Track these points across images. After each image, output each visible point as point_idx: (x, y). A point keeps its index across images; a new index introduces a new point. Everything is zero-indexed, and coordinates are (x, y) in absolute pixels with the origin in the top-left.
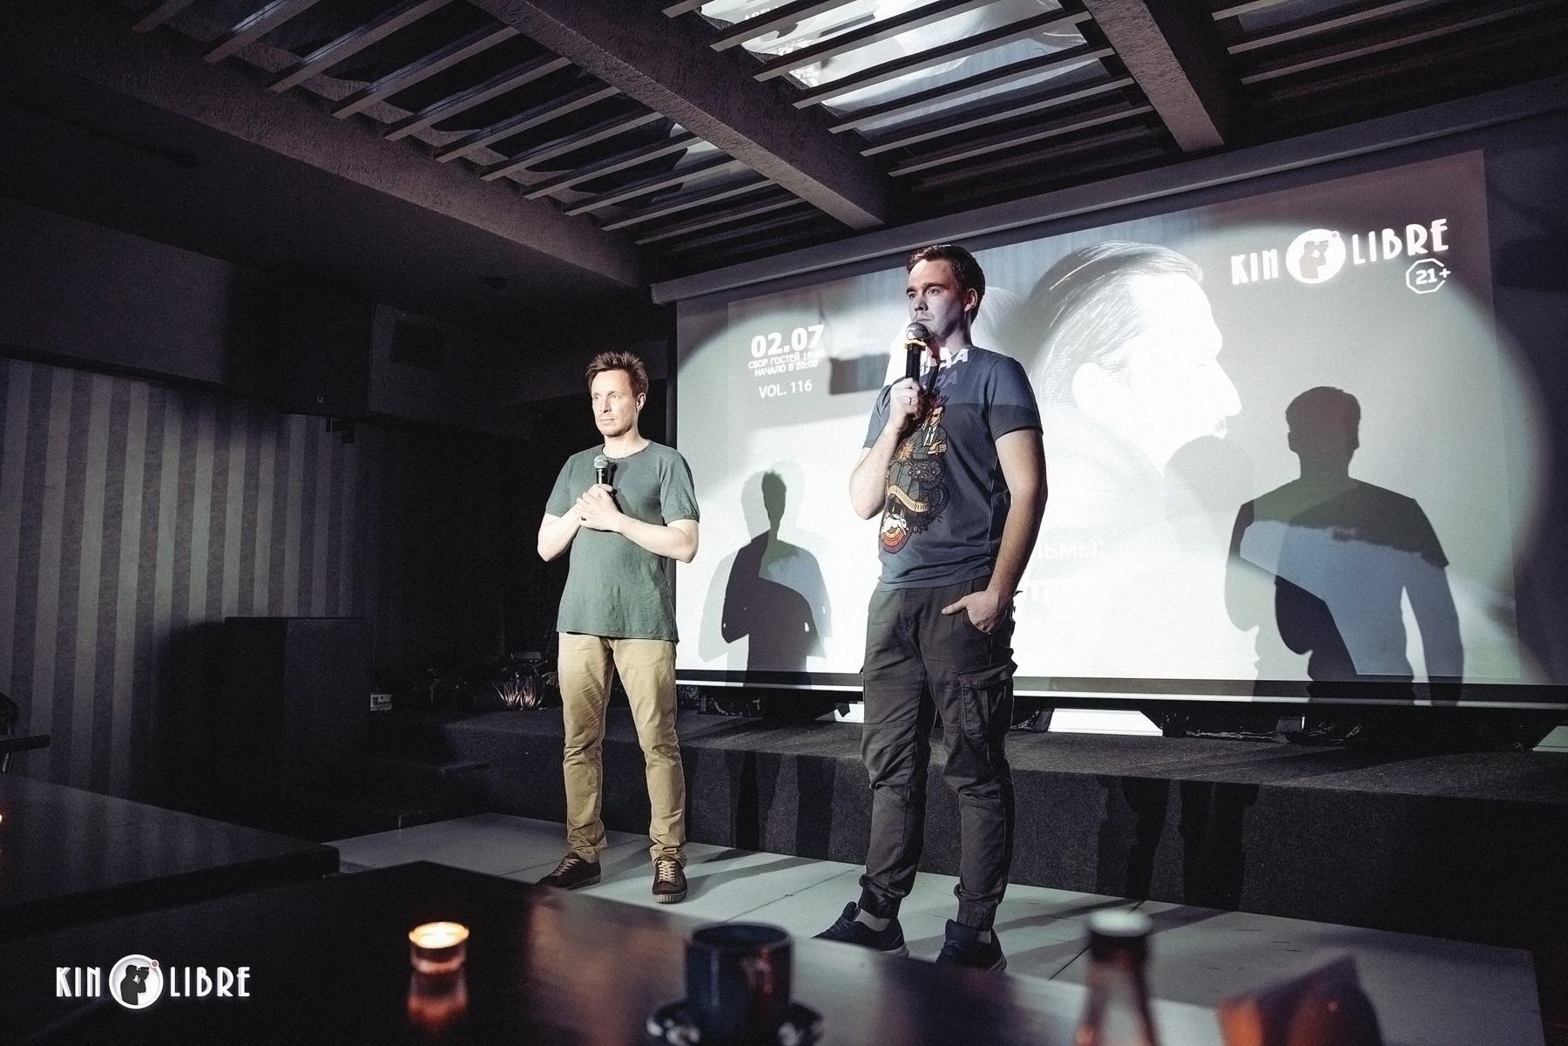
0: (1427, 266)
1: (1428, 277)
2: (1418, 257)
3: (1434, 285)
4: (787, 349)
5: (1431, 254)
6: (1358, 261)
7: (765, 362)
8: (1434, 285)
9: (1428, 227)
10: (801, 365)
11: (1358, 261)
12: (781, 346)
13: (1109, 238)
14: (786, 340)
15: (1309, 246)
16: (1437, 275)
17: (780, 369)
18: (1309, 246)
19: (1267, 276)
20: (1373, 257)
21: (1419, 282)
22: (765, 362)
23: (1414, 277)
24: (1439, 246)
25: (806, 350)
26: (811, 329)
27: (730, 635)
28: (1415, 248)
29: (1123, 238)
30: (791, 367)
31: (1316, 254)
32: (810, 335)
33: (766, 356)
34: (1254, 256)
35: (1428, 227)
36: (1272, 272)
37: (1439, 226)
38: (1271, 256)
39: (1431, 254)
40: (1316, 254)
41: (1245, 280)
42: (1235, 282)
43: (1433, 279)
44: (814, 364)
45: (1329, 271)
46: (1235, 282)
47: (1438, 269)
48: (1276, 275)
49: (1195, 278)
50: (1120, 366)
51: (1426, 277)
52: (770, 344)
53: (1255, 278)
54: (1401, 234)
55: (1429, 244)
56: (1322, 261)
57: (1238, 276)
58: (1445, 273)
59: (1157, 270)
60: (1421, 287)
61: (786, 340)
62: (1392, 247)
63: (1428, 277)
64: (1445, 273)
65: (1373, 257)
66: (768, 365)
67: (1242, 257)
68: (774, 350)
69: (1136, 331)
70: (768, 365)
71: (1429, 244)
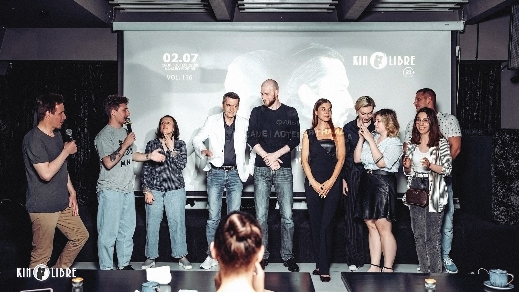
0: (409, 69)
1: (409, 73)
2: (407, 66)
3: (410, 75)
4: (181, 61)
7: (170, 65)
8: (410, 75)
9: (410, 58)
10: (187, 69)
11: (391, 64)
12: (178, 59)
14: (180, 57)
15: (377, 57)
16: (412, 74)
17: (178, 69)
18: (377, 57)
19: (364, 64)
20: (395, 64)
21: (406, 74)
22: (170, 65)
23: (405, 72)
24: (412, 64)
25: (190, 63)
26: (192, 54)
28: (406, 63)
30: (182, 69)
31: (379, 60)
32: (192, 57)
33: (170, 62)
34: (360, 57)
35: (410, 58)
36: (365, 63)
37: (413, 58)
39: (410, 66)
40: (379, 60)
41: (357, 64)
42: (354, 64)
43: (410, 74)
44: (193, 69)
45: (382, 66)
46: (354, 64)
47: (412, 71)
48: (367, 64)
49: (342, 61)
50: (315, 87)
51: (408, 72)
52: (172, 58)
53: (360, 64)
54: (403, 58)
55: (410, 63)
56: (380, 62)
57: (355, 62)
58: (413, 72)
59: (330, 56)
60: (407, 75)
61: (180, 57)
62: (400, 61)
63: (409, 73)
64: (413, 72)
66: (171, 67)
68: (174, 61)
69: (322, 76)
70: (171, 67)
71: (410, 63)
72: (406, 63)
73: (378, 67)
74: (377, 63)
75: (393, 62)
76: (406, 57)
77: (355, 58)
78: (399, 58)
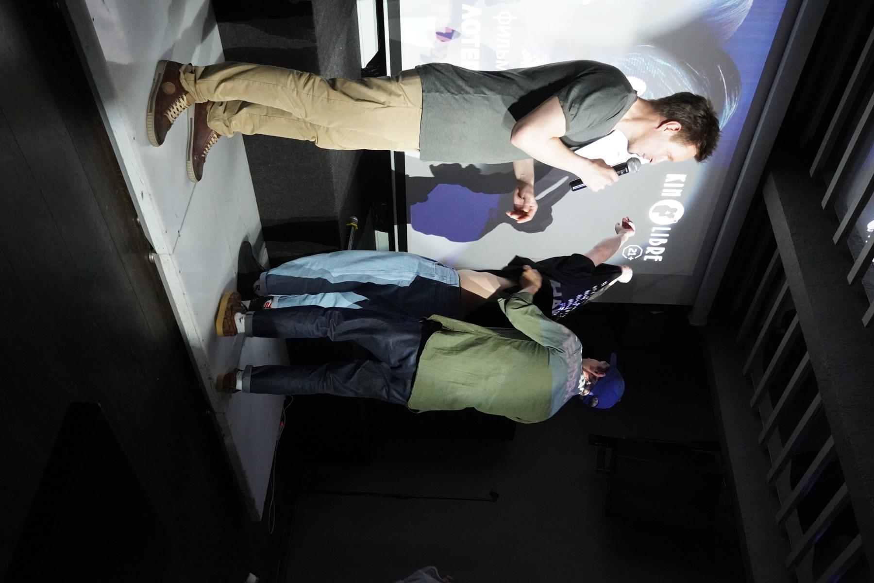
0: (638, 253)
2: (645, 250)
5: (644, 254)
6: (654, 229)
8: (626, 255)
11: (654, 229)
13: (738, 109)
15: (675, 210)
18: (675, 210)
19: (664, 190)
23: (634, 248)
24: (646, 258)
27: (370, 245)
28: (649, 250)
29: (734, 116)
31: (668, 213)
34: (682, 185)
36: (665, 193)
38: (678, 193)
39: (644, 254)
40: (668, 213)
41: (667, 180)
43: (629, 254)
45: (654, 216)
46: (668, 176)
47: (634, 256)
48: (663, 194)
53: (666, 185)
54: (662, 245)
55: (650, 254)
56: (662, 214)
57: (671, 177)
58: (631, 259)
65: (652, 235)
67: (683, 180)
71: (650, 254)
72: (649, 250)
73: (653, 211)
74: (662, 211)
75: (657, 232)
76: (663, 250)
77: (683, 177)
78: (665, 241)
